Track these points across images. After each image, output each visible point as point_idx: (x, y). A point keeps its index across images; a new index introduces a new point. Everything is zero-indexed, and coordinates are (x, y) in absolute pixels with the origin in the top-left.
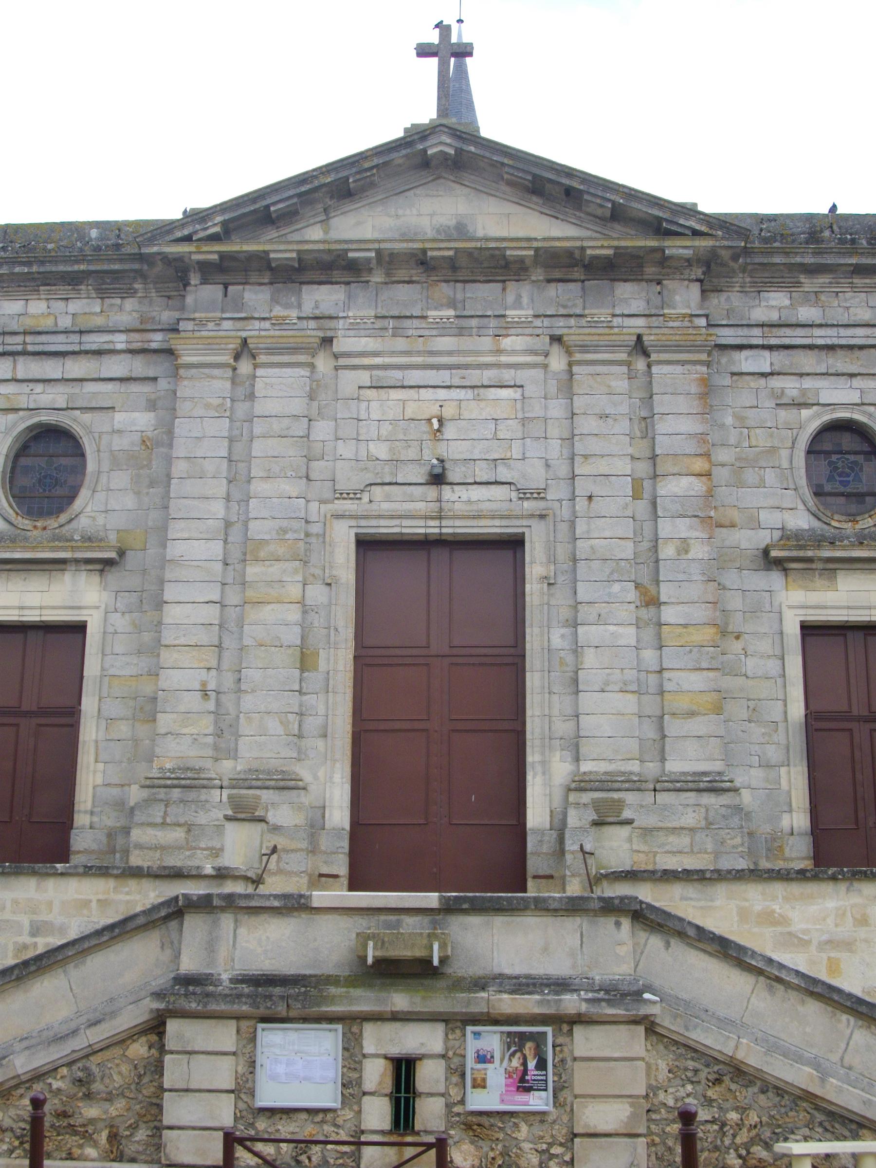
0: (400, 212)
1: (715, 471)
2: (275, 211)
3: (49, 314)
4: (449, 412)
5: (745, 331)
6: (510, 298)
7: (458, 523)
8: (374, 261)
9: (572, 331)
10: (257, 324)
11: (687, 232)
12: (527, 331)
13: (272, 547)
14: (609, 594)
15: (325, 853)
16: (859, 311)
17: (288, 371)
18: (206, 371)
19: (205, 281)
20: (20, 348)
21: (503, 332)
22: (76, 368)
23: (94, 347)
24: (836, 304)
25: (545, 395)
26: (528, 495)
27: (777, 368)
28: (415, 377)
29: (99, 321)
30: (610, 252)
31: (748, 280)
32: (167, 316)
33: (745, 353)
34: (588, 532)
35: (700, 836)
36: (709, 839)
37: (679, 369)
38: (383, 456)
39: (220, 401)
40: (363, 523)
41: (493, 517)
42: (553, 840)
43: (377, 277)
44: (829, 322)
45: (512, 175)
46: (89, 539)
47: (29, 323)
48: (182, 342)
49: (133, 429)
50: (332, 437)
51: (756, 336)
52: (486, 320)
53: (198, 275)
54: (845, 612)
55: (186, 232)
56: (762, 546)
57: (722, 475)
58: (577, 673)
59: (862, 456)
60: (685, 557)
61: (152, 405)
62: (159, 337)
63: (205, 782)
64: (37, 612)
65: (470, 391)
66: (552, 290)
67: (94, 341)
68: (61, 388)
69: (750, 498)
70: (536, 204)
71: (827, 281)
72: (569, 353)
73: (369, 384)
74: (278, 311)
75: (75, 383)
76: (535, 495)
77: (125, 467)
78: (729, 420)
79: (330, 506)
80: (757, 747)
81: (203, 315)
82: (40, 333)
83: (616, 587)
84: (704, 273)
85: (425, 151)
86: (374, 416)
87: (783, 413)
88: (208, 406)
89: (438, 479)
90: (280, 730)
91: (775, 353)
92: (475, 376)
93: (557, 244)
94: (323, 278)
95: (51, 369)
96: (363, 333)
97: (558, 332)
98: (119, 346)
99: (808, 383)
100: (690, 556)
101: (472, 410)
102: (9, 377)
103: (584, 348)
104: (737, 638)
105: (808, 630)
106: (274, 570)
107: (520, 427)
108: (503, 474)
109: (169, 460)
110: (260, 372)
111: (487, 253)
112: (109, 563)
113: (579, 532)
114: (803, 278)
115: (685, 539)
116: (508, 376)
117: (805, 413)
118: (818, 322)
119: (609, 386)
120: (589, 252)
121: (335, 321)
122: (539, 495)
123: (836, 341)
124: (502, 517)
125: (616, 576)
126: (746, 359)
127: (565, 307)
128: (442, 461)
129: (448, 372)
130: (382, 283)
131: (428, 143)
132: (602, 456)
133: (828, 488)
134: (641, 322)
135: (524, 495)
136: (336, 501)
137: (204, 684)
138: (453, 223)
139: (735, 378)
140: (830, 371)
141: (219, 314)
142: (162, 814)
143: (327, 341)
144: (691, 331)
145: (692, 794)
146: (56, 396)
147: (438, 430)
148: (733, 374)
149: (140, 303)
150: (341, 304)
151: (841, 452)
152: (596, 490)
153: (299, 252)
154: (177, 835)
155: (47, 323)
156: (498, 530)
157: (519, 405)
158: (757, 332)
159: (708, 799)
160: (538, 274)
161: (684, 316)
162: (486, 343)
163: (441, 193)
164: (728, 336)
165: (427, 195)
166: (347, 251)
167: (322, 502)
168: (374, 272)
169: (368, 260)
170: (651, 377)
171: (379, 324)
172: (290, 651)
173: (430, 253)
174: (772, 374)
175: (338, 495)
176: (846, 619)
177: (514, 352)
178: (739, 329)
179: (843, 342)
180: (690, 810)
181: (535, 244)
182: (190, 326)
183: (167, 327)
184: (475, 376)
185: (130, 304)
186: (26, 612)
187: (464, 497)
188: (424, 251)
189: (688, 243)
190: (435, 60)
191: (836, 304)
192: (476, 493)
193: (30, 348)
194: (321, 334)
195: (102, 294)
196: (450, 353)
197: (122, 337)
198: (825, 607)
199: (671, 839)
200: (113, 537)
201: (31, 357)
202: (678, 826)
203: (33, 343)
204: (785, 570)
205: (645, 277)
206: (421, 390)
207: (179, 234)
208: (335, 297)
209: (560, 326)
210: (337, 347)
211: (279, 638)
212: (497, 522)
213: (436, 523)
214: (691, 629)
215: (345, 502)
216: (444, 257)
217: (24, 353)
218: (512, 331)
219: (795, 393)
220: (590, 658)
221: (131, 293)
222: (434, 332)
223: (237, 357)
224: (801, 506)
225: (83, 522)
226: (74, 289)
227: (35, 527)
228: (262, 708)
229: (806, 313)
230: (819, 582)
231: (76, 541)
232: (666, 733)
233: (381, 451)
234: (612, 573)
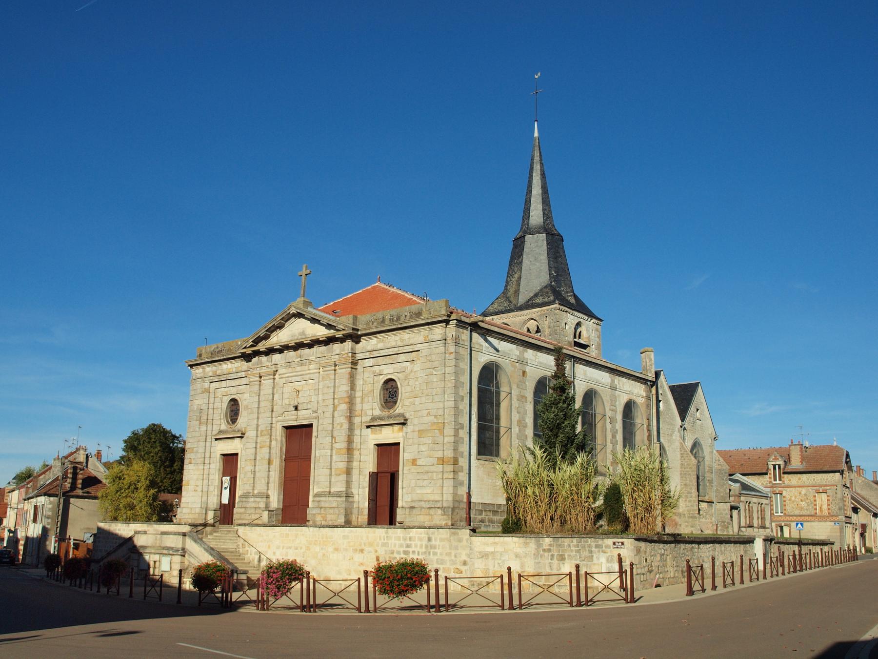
22: (237, 382)
28: (294, 379)
35: (336, 509)
40: (283, 423)
41: (306, 419)
51: (367, 355)
67: (239, 375)
69: (366, 406)
79: (277, 419)
95: (233, 383)
98: (244, 376)
115: (342, 423)
117: (381, 377)
119: (330, 378)
124: (308, 419)
127: (323, 354)
131: (290, 311)
138: (302, 331)
141: (256, 366)
145: (335, 498)
146: (234, 390)
154: (243, 510)
158: (368, 353)
159: (339, 499)
161: (346, 353)
162: (306, 367)
167: (276, 418)
194: (275, 369)
197: (244, 373)
199: (330, 510)
207: (244, 346)
212: (308, 421)
213: (296, 422)
219: (377, 371)
222: (297, 366)
225: (239, 425)
229: (380, 346)
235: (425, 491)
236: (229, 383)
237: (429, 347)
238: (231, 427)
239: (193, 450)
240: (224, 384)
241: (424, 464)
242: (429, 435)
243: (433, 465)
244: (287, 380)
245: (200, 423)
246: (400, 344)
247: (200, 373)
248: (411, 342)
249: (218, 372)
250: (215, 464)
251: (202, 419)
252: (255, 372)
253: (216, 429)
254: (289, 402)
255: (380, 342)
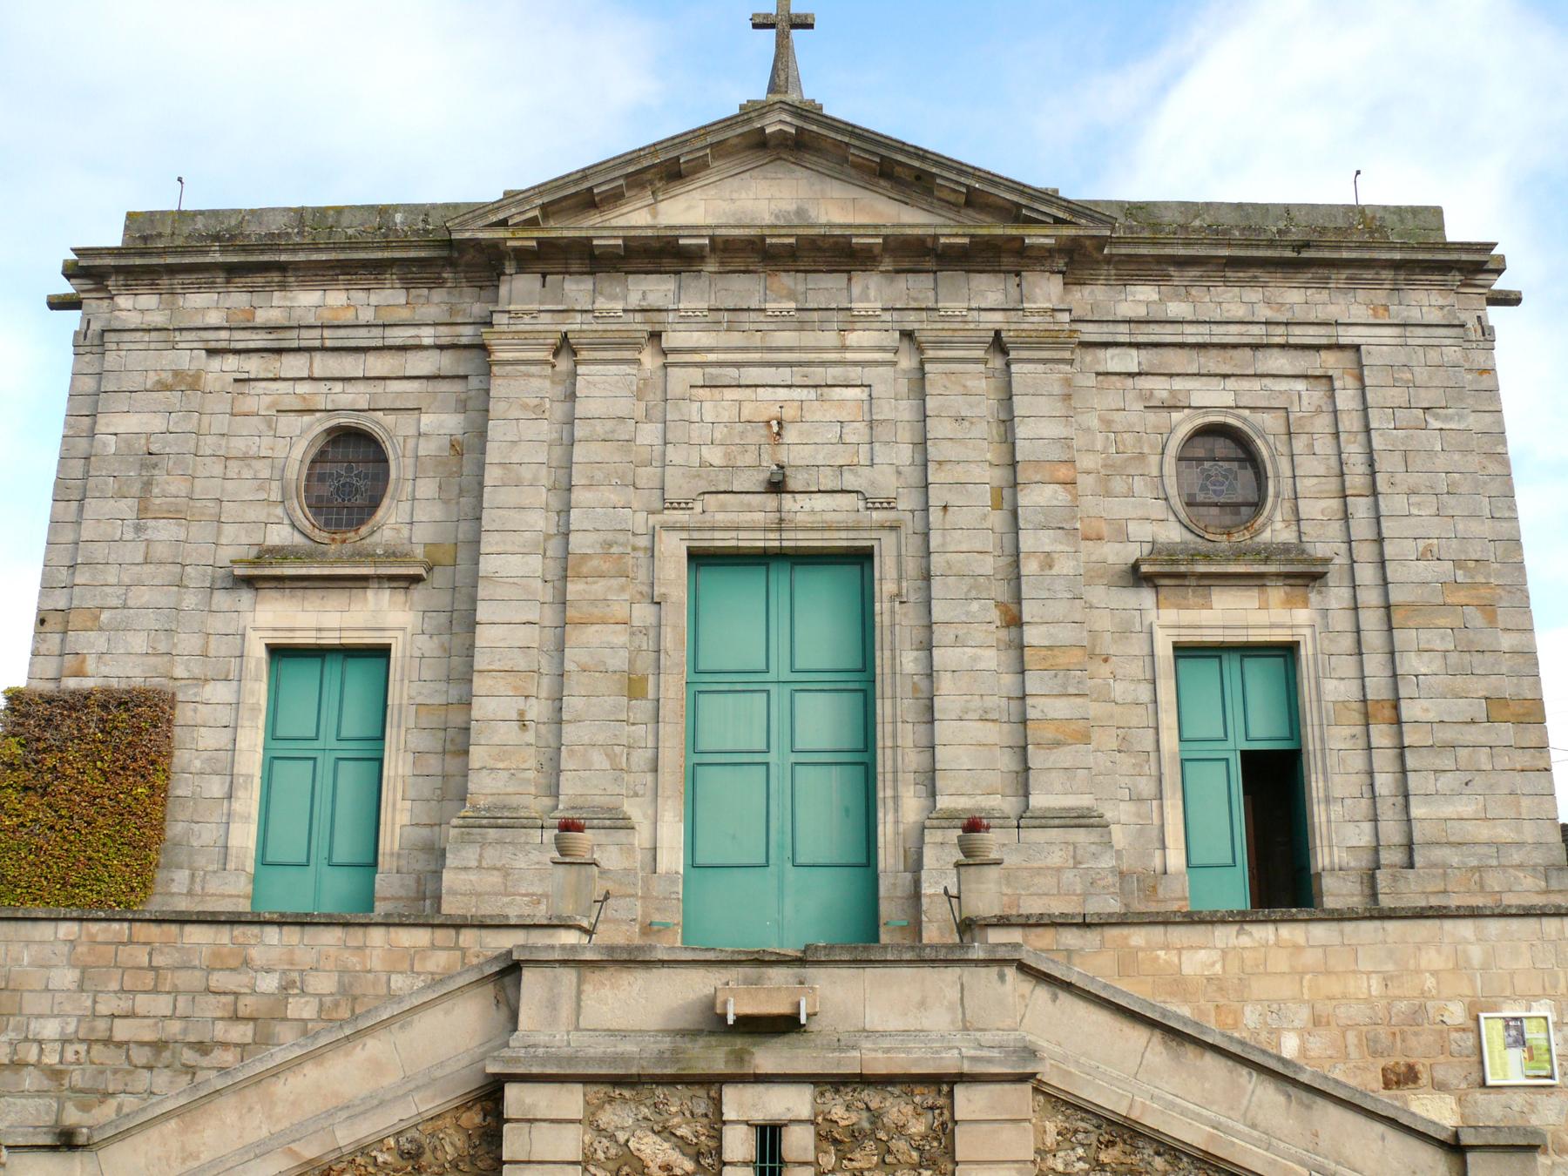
0: (735, 196)
1: (1081, 479)
2: (599, 194)
3: (349, 306)
4: (789, 413)
5: (1111, 328)
6: (856, 289)
7: (800, 535)
8: (708, 249)
9: (925, 326)
10: (579, 318)
11: (1048, 220)
12: (878, 325)
13: (595, 562)
14: (967, 613)
15: (657, 898)
16: (1233, 307)
17: (613, 368)
18: (522, 368)
19: (521, 270)
20: (317, 343)
21: (849, 326)
22: (378, 365)
23: (399, 342)
24: (1207, 299)
25: (896, 394)
26: (878, 505)
27: (1145, 368)
29: (404, 314)
30: (966, 240)
31: (1113, 272)
32: (478, 309)
33: (1111, 352)
34: (943, 545)
36: (1078, 879)
37: (1040, 368)
38: (716, 462)
39: (537, 401)
40: (696, 535)
41: (838, 529)
42: (907, 883)
43: (711, 266)
44: (1201, 319)
45: (859, 156)
46: (393, 555)
47: (327, 317)
48: (496, 336)
49: (442, 432)
50: (660, 441)
51: (1122, 333)
52: (829, 313)
53: (513, 263)
54: (1220, 632)
55: (501, 216)
56: (1132, 561)
57: (1086, 483)
58: (932, 699)
59: (1236, 464)
60: (1047, 572)
61: (462, 406)
62: (469, 330)
63: (525, 821)
64: (337, 634)
65: (812, 391)
66: (903, 283)
67: (398, 336)
68: (361, 387)
69: (1117, 508)
70: (883, 188)
71: (1198, 274)
72: (921, 350)
73: (702, 383)
74: (602, 304)
75: (377, 382)
76: (885, 505)
77: (432, 474)
78: (1094, 423)
79: (659, 517)
80: (1127, 780)
81: (519, 307)
82: (338, 327)
83: (975, 606)
84: (1066, 264)
85: (762, 129)
86: (708, 418)
87: (1152, 417)
88: (525, 407)
89: (776, 487)
90: (606, 765)
91: (1143, 352)
92: (818, 375)
93: (908, 231)
94: (650, 267)
96: (694, 327)
97: (909, 327)
98: (427, 341)
99: (1178, 384)
100: (1054, 572)
101: (817, 413)
102: (305, 375)
103: (939, 344)
104: (1106, 660)
105: (1183, 651)
106: (599, 587)
107: (867, 430)
108: (850, 481)
109: (481, 466)
110: (581, 369)
111: (831, 240)
112: (416, 579)
113: (933, 544)
114: (1172, 270)
116: (855, 374)
117: (1176, 416)
118: (1189, 319)
119: (964, 386)
120: (942, 240)
121: (665, 314)
122: (888, 504)
123: (1207, 339)
124: (847, 529)
125: (973, 594)
126: (1112, 358)
127: (915, 300)
128: (781, 467)
129: (788, 370)
130: (715, 273)
131: (767, 121)
132: (958, 463)
133: (1200, 498)
134: (999, 316)
135: (872, 504)
136: (666, 512)
137: (521, 713)
139: (1100, 378)
140: (1202, 372)
141: (536, 307)
142: (477, 856)
143: (655, 336)
144: (1052, 327)
147: (778, 434)
148: (1098, 374)
149: (449, 293)
150: (671, 295)
151: (1214, 460)
152: (952, 498)
153: (625, 238)
154: (495, 879)
155: (348, 317)
156: (845, 544)
157: (866, 407)
158: (1124, 328)
160: (887, 264)
161: (1045, 311)
162: (830, 338)
163: (780, 176)
164: (1090, 333)
165: (765, 178)
166: (677, 237)
168: (708, 260)
169: (701, 247)
170: (1010, 377)
171: (712, 317)
172: (617, 676)
173: (768, 241)
174: (1140, 374)
175: (667, 505)
176: (1221, 639)
177: (860, 349)
178: (1105, 325)
179: (1215, 340)
180: (1056, 848)
181: (884, 231)
182: (504, 319)
183: (478, 320)
184: (818, 375)
185: (438, 295)
186: (324, 634)
187: (807, 507)
188: (763, 238)
189: (1048, 232)
190: (773, 32)
191: (1207, 299)
192: (820, 502)
193: (328, 343)
194: (648, 328)
195: (408, 284)
196: (790, 349)
197: (429, 331)
198: (1200, 627)
200: (419, 552)
201: (330, 354)
202: (1043, 865)
203: (331, 338)
204: (1156, 586)
205: (1003, 268)
206: (759, 389)
208: (664, 287)
209: (912, 321)
210: (669, 340)
211: (605, 663)
212: (843, 535)
214: (1056, 652)
215: (675, 512)
216: (783, 245)
217: (324, 349)
218: (858, 326)
219: (1165, 394)
220: (945, 684)
221: (439, 283)
222: (772, 327)
223: (556, 354)
224: (1172, 518)
226: (376, 279)
227: (333, 540)
228: (586, 740)
229: (1176, 309)
230: (1192, 600)
231: (379, 556)
232: (1030, 765)
233: (715, 456)
234: (969, 591)
235: (1448, 810)
236: (325, 365)
237: (1398, 341)
238: (337, 537)
239: (97, 618)
240: (294, 365)
241: (1431, 716)
242: (1441, 622)
243: (1473, 722)
244: (712, 377)
245: (143, 511)
246: (1264, 313)
247: (142, 311)
248: (1320, 314)
249: (262, 317)
250: (235, 683)
251: (156, 491)
252: (520, 328)
253: (235, 545)
254: (727, 455)
255: (1177, 297)
